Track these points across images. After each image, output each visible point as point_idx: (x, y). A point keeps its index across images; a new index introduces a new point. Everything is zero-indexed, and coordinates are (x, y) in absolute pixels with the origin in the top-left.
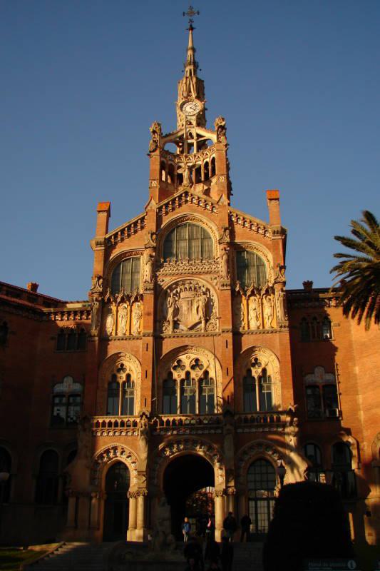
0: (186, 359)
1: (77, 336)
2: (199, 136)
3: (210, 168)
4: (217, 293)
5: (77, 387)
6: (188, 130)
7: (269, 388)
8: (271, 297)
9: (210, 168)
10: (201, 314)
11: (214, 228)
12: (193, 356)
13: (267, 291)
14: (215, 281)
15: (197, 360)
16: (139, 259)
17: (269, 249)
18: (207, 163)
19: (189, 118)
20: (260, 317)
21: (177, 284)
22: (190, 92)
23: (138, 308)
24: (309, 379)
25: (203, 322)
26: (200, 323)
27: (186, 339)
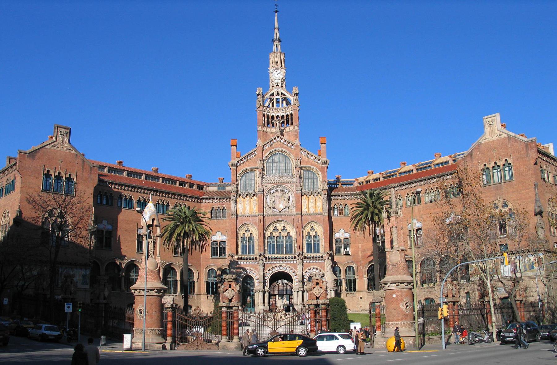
0: (280, 226)
1: (221, 211)
3: (290, 119)
6: (276, 89)
7: (318, 241)
8: (319, 196)
9: (290, 119)
10: (286, 204)
11: (293, 157)
13: (319, 193)
14: (293, 187)
15: (284, 227)
16: (254, 172)
17: (320, 171)
18: (287, 115)
19: (276, 81)
20: (315, 207)
21: (274, 187)
22: (277, 62)
25: (287, 208)
26: (286, 208)
27: (279, 217)
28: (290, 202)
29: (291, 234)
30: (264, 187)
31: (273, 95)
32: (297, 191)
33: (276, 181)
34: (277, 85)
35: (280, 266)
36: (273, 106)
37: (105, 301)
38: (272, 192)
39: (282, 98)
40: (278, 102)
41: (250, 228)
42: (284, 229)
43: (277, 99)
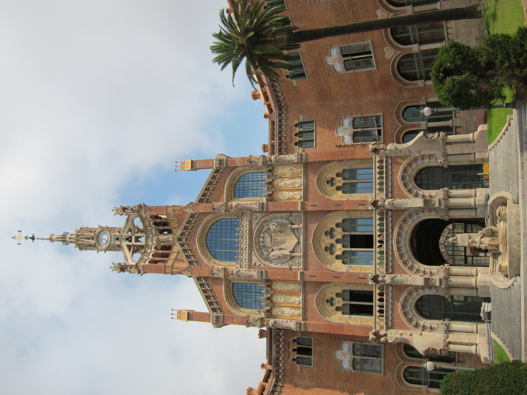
3: (158, 221)
4: (269, 214)
5: (346, 346)
12: (323, 237)
13: (270, 171)
15: (326, 233)
16: (233, 284)
18: (155, 224)
24: (348, 140)
28: (284, 221)
29: (340, 221)
31: (129, 247)
32: (263, 208)
33: (247, 246)
34: (118, 239)
35: (398, 242)
38: (266, 253)
39: (135, 233)
41: (328, 296)
42: (330, 233)
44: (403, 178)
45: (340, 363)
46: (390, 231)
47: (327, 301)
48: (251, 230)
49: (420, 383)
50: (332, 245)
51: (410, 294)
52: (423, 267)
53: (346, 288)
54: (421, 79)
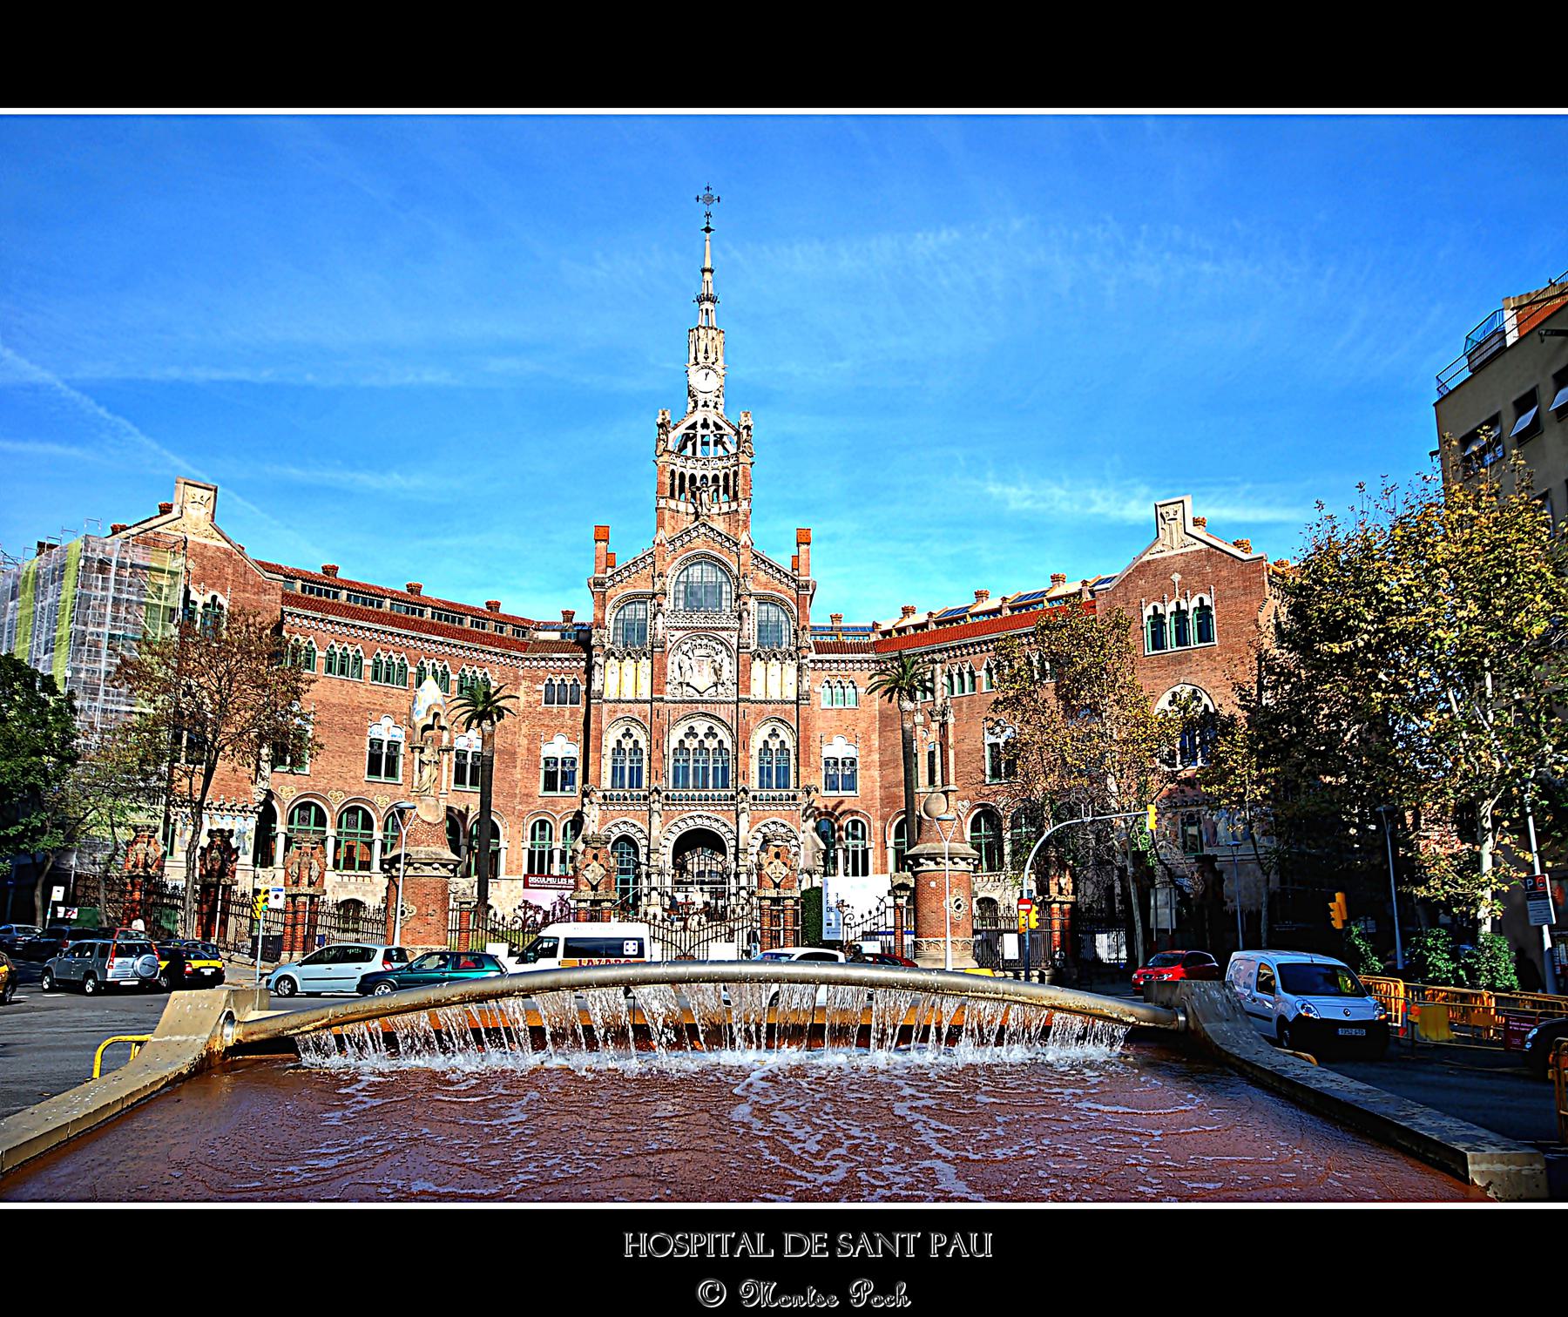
2: (718, 427)
15: (711, 728)
18: (726, 476)
22: (706, 352)
23: (645, 663)
24: (828, 752)
28: (725, 675)
30: (668, 637)
31: (693, 426)
34: (705, 405)
36: (694, 452)
37: (311, 891)
38: (685, 648)
40: (705, 444)
42: (711, 733)
43: (703, 437)
44: (774, 823)
45: (549, 742)
46: (712, 808)
47: (628, 730)
48: (715, 629)
49: (533, 838)
50: (696, 735)
51: (642, 831)
52: (671, 845)
53: (645, 753)
54: (896, 844)
